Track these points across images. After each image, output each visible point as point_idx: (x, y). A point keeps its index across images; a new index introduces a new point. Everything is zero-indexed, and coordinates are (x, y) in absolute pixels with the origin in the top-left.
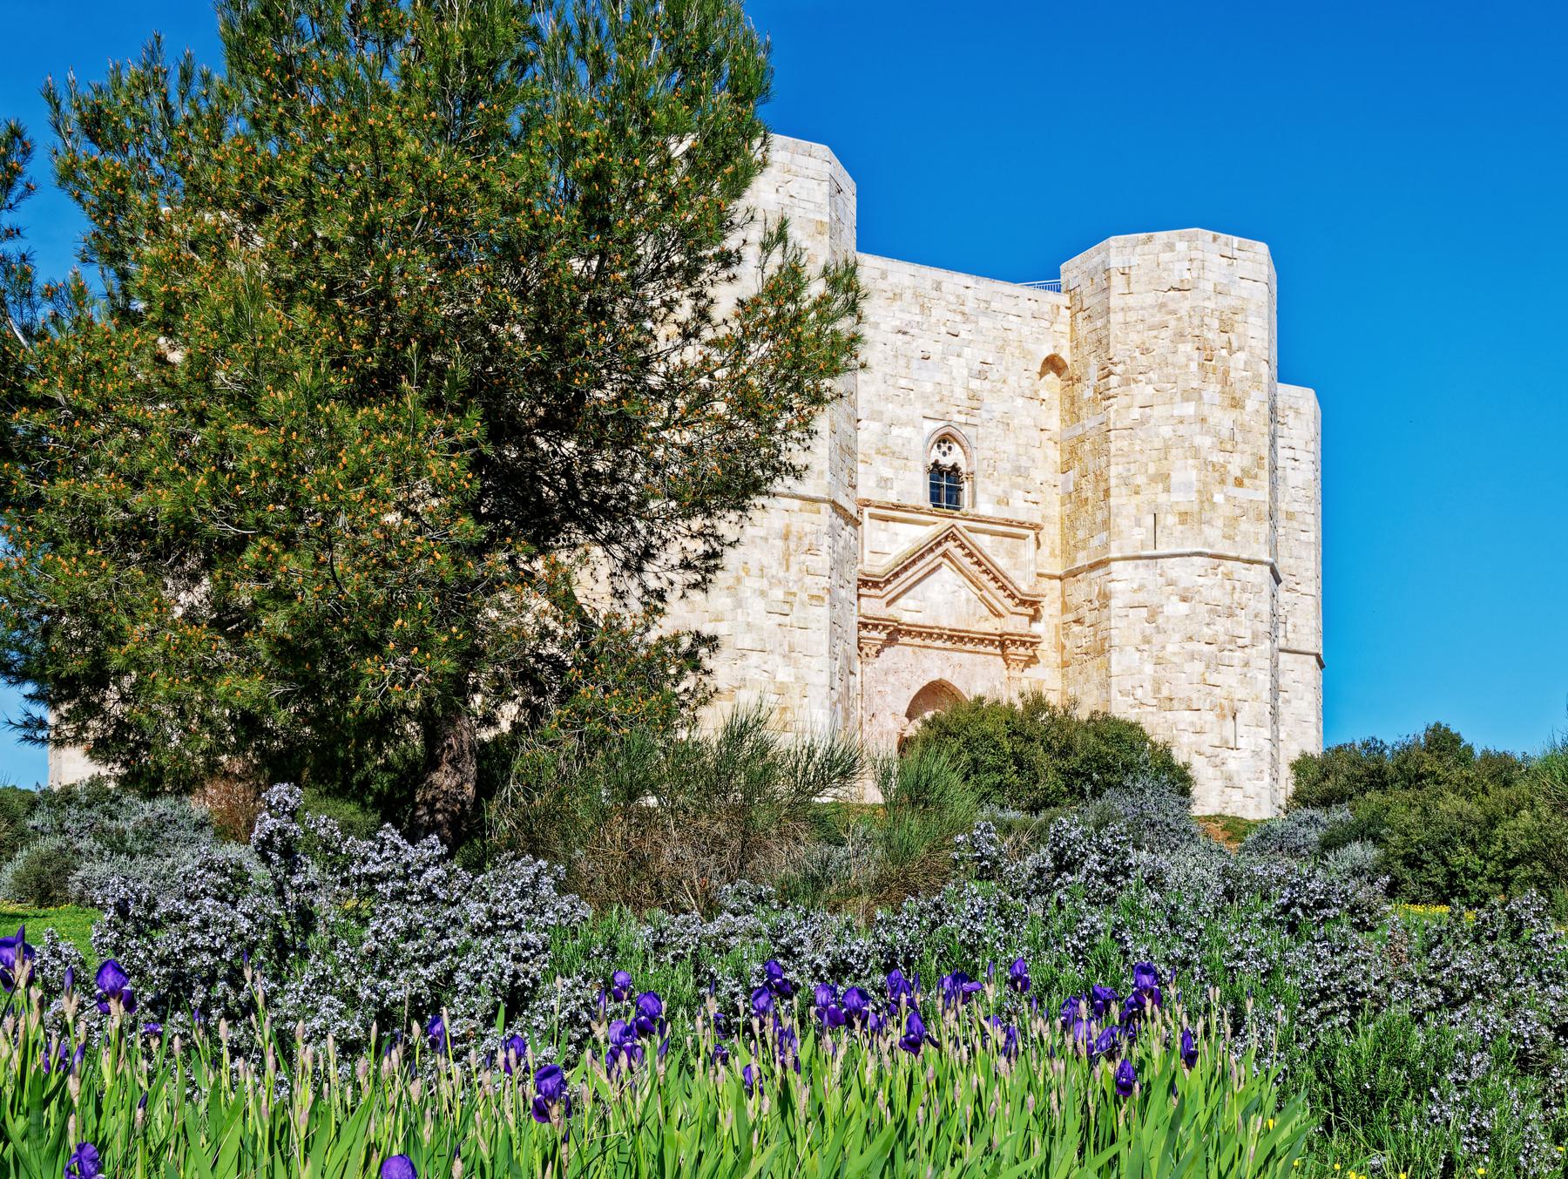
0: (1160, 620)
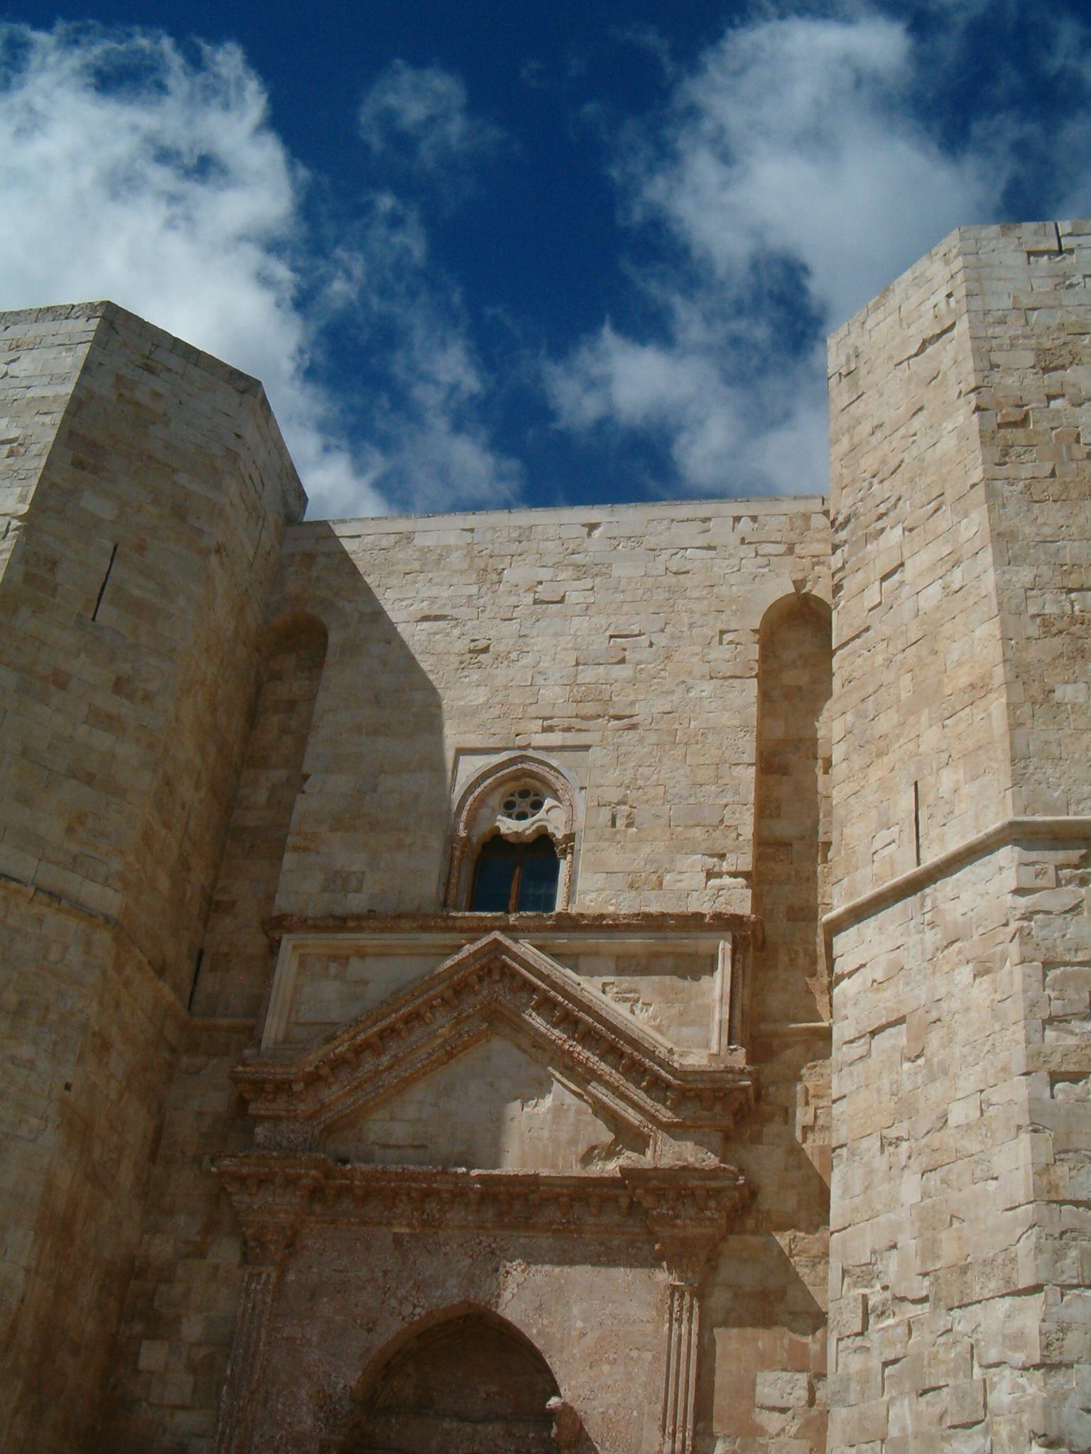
0: (934, 1040)
